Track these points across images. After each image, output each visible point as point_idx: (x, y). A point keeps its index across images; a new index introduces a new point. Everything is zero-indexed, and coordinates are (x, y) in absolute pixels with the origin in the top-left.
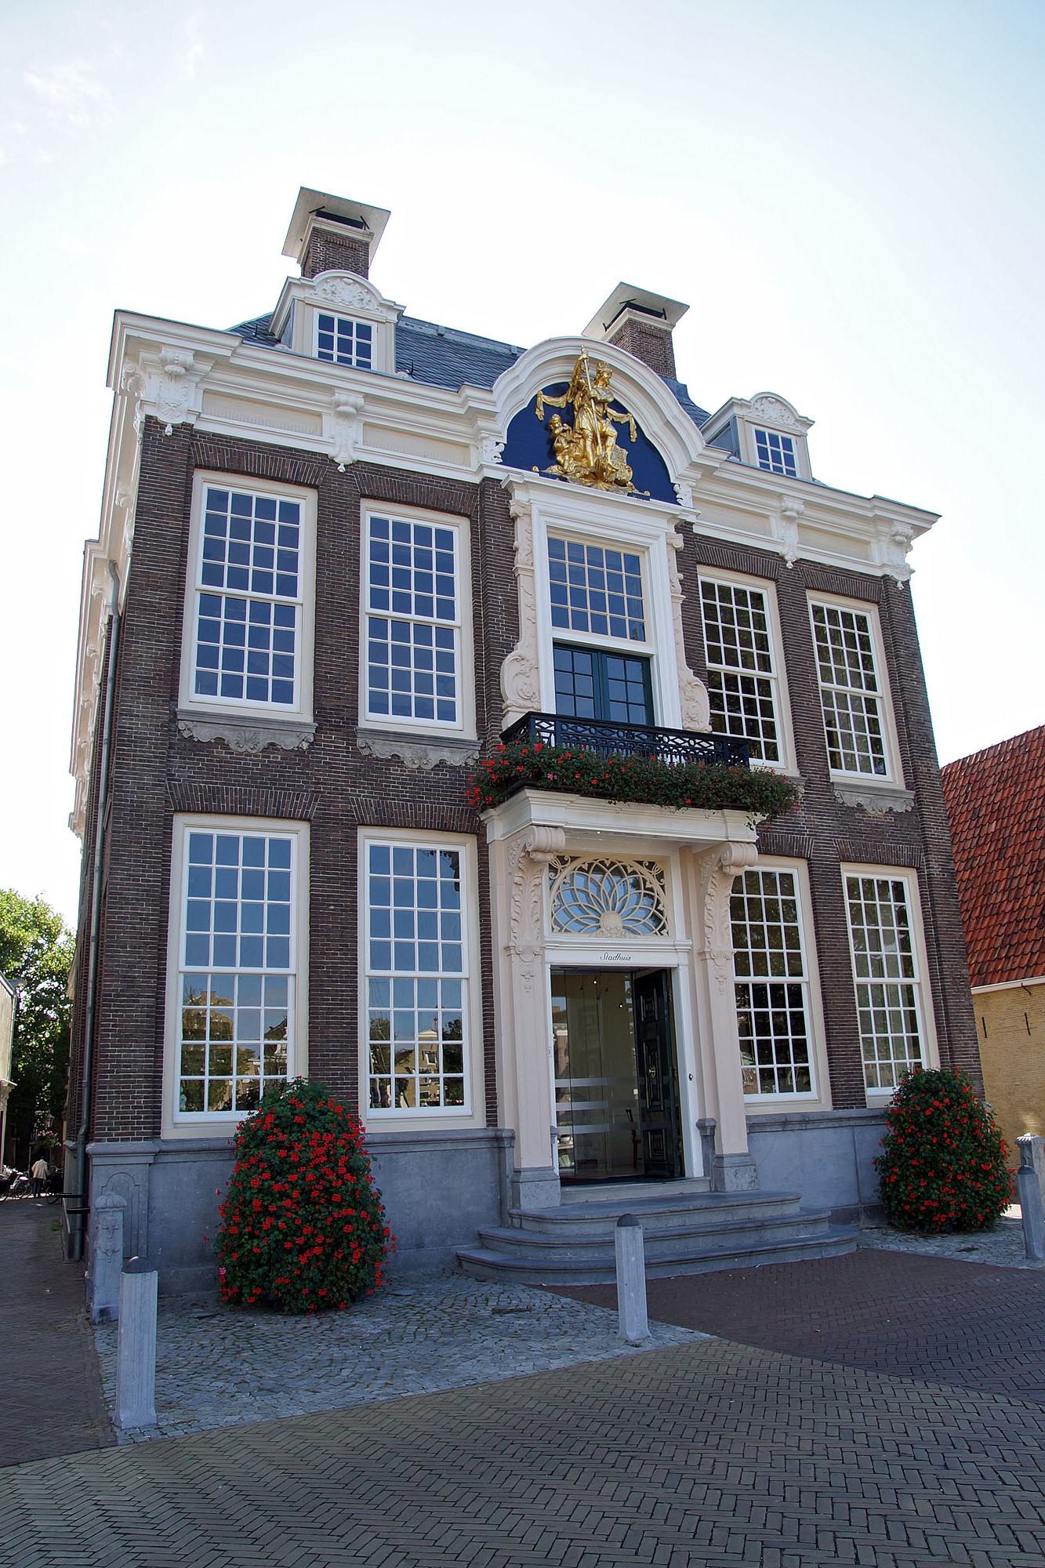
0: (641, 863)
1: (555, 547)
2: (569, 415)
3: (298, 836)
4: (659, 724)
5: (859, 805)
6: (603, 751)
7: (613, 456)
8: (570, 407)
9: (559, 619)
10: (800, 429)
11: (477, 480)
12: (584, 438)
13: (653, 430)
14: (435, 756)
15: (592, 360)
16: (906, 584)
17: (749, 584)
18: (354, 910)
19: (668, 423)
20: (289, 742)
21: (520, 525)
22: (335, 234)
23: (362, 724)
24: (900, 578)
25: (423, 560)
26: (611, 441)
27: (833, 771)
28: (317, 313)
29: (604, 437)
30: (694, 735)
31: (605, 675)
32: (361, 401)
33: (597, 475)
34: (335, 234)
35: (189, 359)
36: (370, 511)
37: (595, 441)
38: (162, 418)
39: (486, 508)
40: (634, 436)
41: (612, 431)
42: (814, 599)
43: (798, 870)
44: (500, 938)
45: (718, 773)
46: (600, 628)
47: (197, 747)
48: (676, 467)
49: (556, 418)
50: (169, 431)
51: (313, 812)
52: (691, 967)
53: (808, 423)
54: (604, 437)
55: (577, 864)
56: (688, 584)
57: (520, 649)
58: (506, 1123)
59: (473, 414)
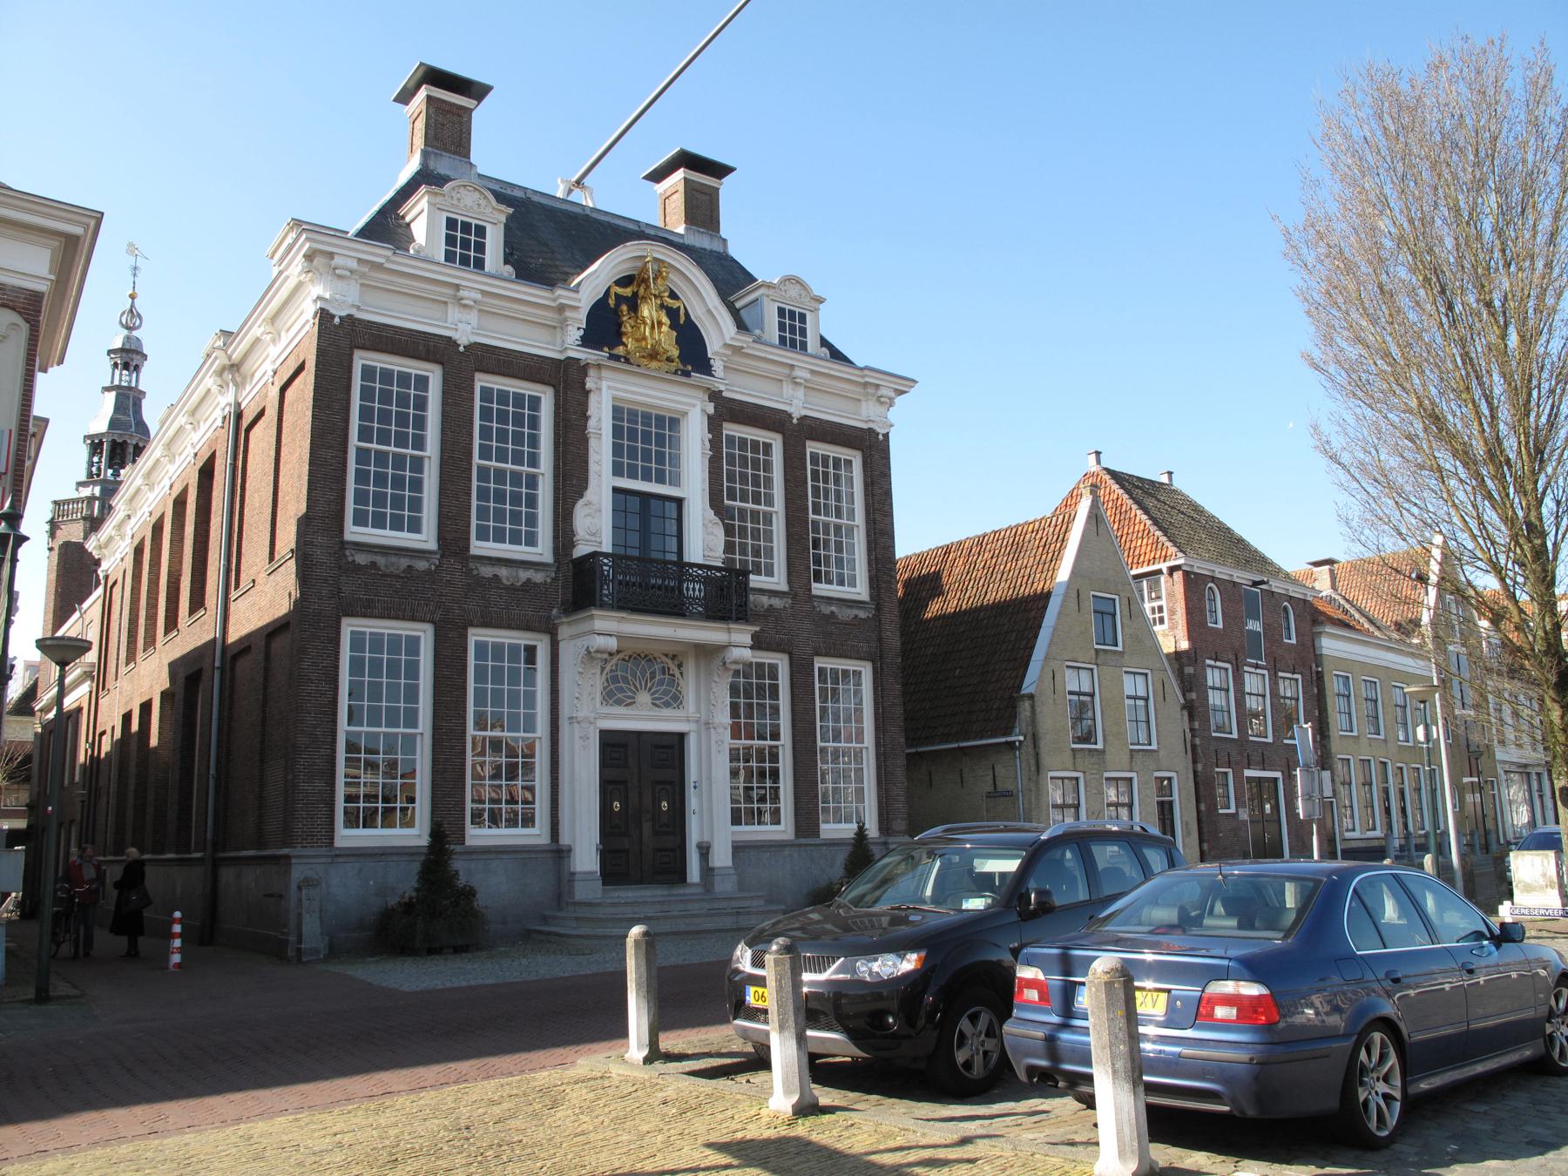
1: (617, 412)
2: (634, 307)
3: (425, 634)
4: (686, 559)
6: (644, 574)
7: (666, 338)
8: (635, 294)
9: (617, 470)
10: (814, 304)
11: (561, 357)
12: (645, 323)
13: (698, 314)
14: (524, 575)
15: (656, 259)
16: (886, 436)
17: (762, 436)
18: (465, 689)
19: (709, 311)
20: (422, 565)
21: (593, 399)
22: (449, 100)
23: (474, 551)
24: (882, 431)
25: (518, 420)
26: (665, 329)
27: (814, 585)
28: (444, 216)
29: (660, 324)
30: (709, 568)
31: (646, 515)
32: (478, 296)
33: (653, 355)
34: (449, 100)
35: (354, 265)
36: (482, 381)
37: (653, 327)
38: (332, 311)
39: (567, 380)
41: (665, 319)
42: (812, 447)
43: (781, 662)
44: (565, 710)
45: (726, 595)
46: (647, 477)
47: (358, 568)
48: (713, 346)
49: (624, 308)
50: (337, 320)
51: (437, 617)
52: (698, 732)
53: (820, 301)
54: (660, 324)
55: (621, 656)
56: (715, 444)
57: (590, 494)
58: (565, 840)
59: (561, 308)
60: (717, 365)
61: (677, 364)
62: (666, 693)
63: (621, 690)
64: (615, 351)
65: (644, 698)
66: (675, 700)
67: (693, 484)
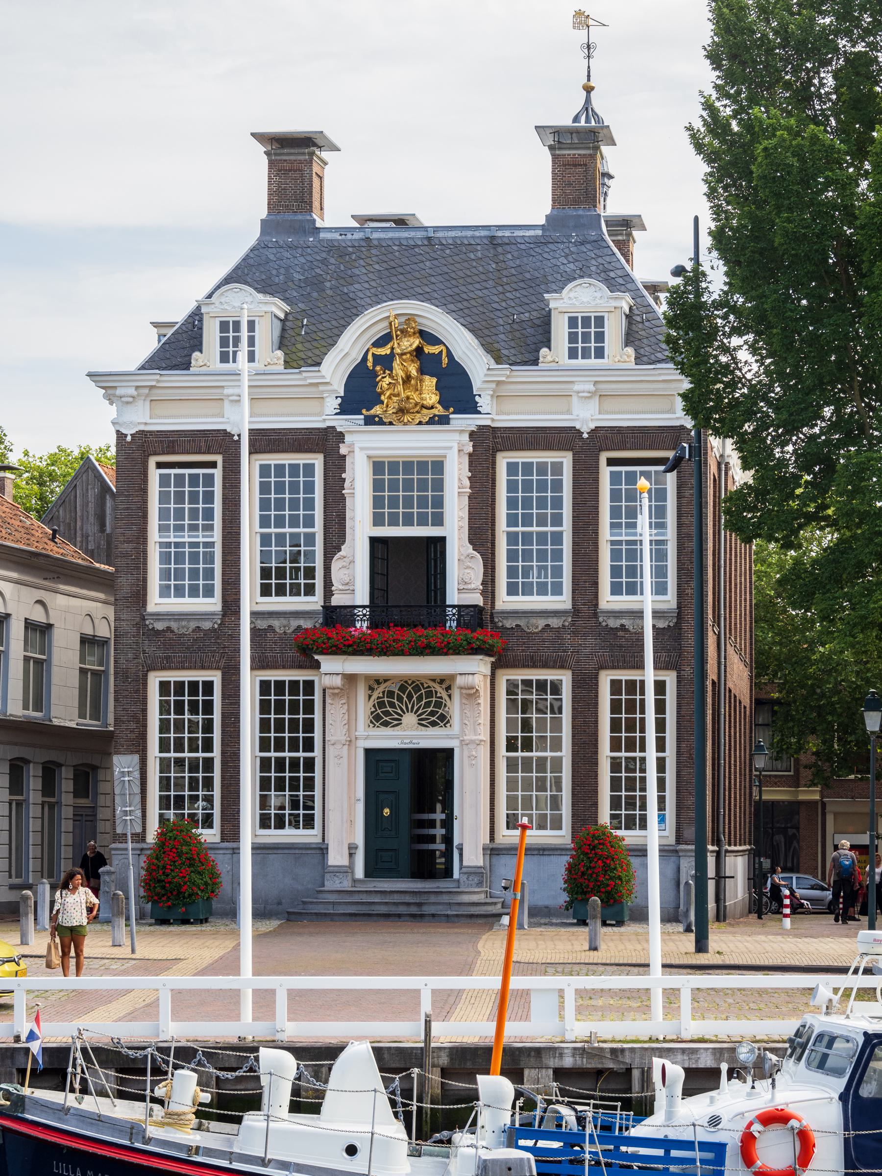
0: (434, 680)
1: (378, 467)
5: (622, 625)
40: (445, 361)
60: (484, 402)
61: (439, 410)
62: (432, 714)
63: (387, 713)
64: (372, 412)
65: (410, 719)
66: (444, 720)
67: (454, 527)
